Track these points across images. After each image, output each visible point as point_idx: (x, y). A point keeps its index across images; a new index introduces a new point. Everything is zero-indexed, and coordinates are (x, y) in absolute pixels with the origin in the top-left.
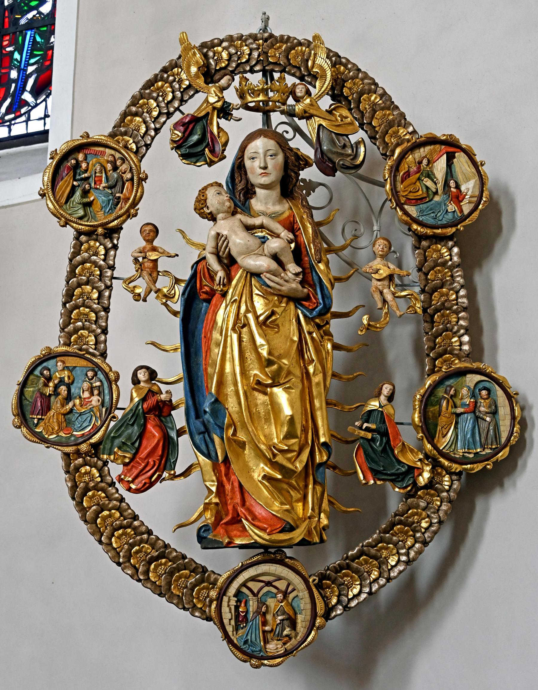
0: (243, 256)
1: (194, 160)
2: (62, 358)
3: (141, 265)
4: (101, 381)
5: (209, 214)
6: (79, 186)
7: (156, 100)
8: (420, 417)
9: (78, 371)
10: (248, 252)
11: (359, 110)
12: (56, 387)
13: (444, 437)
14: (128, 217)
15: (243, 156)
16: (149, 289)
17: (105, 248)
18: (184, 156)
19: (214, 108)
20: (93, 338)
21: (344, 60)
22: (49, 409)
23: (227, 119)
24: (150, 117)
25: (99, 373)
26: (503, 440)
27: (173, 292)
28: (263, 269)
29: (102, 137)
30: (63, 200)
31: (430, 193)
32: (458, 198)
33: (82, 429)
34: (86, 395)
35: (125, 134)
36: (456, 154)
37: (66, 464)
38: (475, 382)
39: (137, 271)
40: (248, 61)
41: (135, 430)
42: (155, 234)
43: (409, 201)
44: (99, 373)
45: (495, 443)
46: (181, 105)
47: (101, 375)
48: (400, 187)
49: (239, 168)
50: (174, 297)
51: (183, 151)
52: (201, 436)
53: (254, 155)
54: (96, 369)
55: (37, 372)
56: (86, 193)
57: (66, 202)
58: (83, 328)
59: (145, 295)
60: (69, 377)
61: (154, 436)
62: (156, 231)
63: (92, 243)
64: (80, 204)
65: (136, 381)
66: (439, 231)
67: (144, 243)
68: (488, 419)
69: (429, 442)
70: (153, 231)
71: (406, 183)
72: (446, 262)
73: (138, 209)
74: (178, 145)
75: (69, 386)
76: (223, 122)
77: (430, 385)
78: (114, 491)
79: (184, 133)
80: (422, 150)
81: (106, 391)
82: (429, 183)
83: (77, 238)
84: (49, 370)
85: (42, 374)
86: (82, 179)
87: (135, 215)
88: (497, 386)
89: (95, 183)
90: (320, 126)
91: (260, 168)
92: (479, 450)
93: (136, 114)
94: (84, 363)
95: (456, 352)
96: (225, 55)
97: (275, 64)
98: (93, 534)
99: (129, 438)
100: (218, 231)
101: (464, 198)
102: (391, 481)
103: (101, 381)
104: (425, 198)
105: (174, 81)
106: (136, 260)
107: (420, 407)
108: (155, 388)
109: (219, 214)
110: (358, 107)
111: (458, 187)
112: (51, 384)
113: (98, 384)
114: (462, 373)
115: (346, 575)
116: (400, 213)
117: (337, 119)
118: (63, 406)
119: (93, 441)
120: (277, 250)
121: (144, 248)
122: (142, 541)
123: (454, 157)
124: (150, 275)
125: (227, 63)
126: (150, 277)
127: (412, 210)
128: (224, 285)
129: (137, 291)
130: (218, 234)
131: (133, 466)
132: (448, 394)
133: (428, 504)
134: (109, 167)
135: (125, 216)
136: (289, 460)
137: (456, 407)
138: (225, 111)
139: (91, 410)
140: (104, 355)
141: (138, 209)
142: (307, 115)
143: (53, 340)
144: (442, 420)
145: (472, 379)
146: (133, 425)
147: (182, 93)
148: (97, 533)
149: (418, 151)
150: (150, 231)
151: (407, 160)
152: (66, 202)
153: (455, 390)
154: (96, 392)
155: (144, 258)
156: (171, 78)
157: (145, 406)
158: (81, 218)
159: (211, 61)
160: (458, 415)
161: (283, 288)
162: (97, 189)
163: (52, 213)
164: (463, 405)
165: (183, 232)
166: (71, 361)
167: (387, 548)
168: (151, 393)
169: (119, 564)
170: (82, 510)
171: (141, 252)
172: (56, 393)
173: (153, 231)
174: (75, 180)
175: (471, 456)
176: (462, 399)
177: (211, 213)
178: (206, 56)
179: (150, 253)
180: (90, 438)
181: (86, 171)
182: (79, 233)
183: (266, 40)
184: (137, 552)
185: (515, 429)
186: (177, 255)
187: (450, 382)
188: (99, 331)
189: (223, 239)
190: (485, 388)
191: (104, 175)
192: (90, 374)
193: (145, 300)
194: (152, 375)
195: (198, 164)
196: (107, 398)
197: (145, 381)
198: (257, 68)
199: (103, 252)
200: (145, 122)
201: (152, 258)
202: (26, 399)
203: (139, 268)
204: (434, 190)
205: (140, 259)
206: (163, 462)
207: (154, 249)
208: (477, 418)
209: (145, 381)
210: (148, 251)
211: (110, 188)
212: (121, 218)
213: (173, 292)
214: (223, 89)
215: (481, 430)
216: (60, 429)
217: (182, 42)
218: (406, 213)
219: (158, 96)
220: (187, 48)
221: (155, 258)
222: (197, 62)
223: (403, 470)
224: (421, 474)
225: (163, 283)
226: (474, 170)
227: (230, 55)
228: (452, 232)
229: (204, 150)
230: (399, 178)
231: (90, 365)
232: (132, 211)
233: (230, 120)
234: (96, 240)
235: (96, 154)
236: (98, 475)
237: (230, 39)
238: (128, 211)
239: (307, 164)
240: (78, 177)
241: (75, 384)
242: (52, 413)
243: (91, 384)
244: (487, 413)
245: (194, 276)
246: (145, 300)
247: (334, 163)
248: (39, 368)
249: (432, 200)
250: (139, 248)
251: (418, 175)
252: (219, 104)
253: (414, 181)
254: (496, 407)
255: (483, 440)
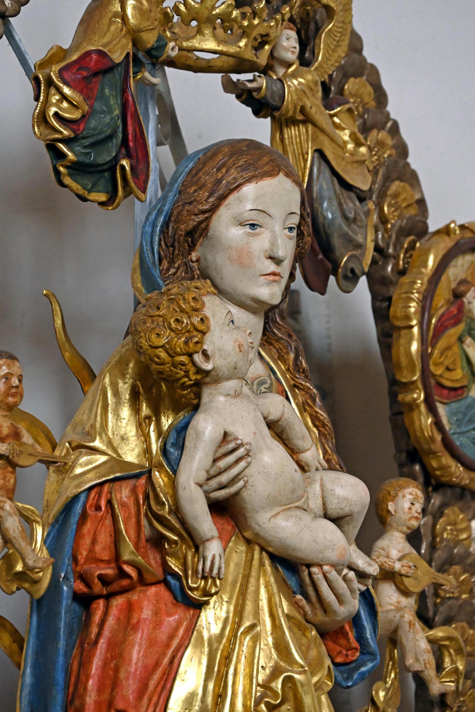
0: (278, 509)
5: (199, 371)
10: (293, 502)
15: (214, 209)
91: (271, 258)
100: (230, 429)
109: (229, 378)
189: (241, 451)
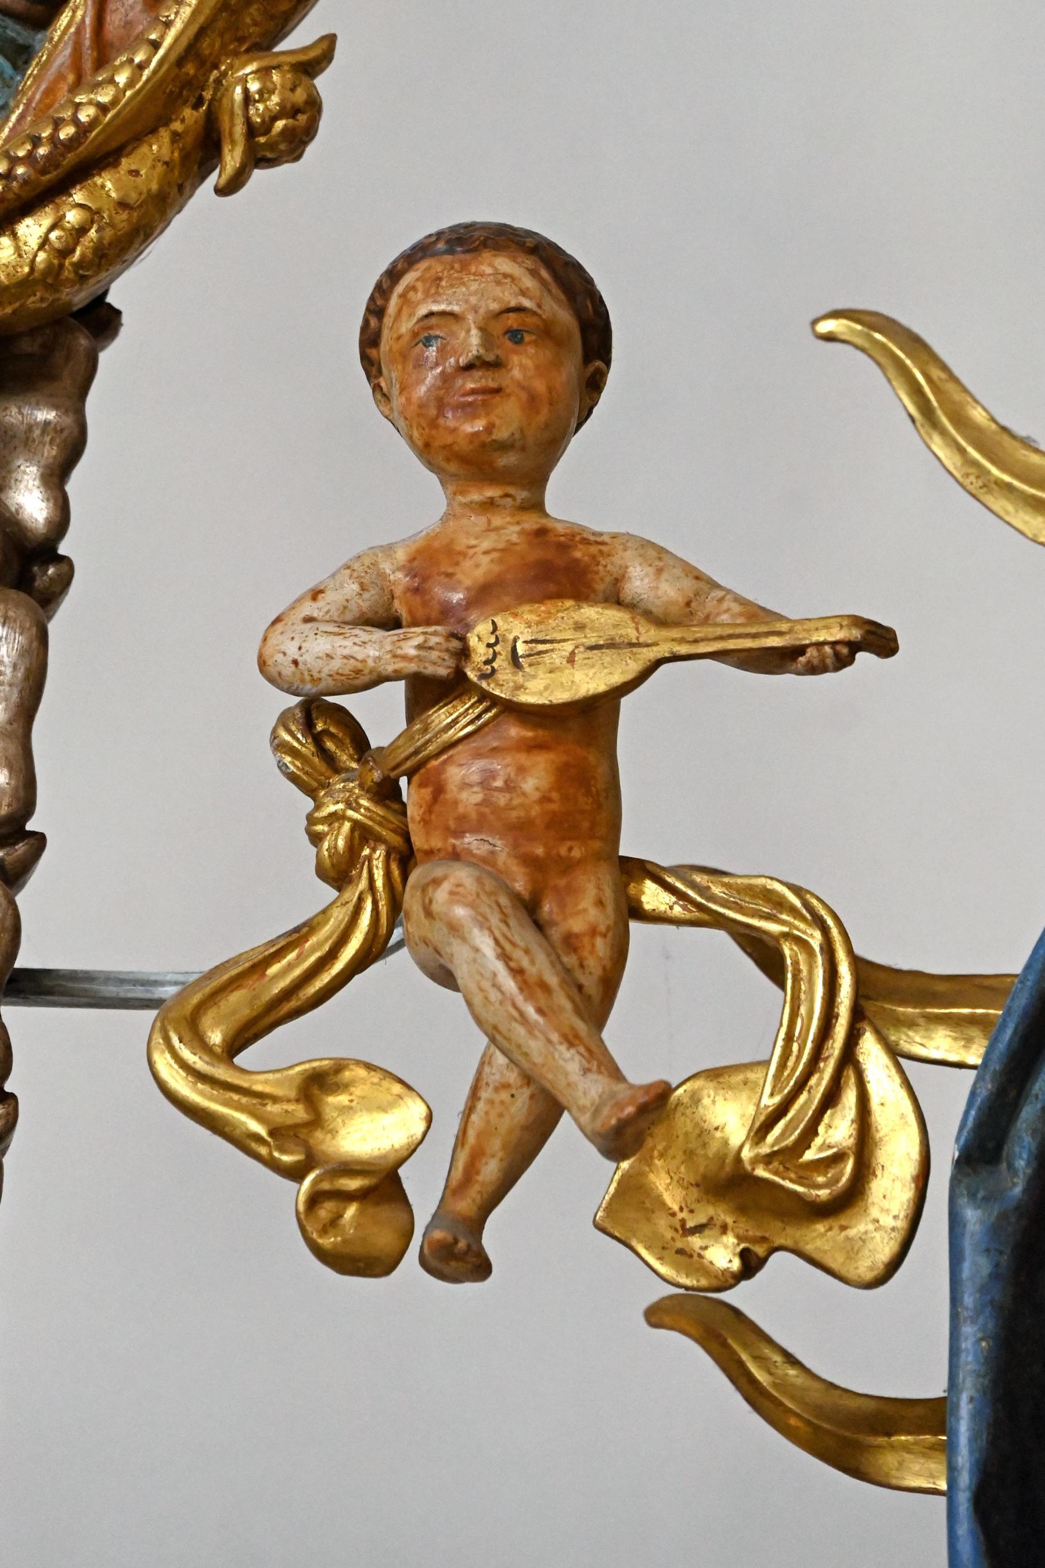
3: (387, 793)
14: (203, 152)
16: (520, 1107)
27: (839, 1130)
39: (338, 873)
42: (570, 371)
50: (851, 1197)
59: (453, 1191)
62: (577, 328)
67: (413, 502)
70: (547, 332)
73: (330, 40)
87: (287, 137)
121: (429, 561)
124: (530, 908)
126: (523, 935)
129: (365, 1133)
135: (159, 147)
141: (330, 40)
150: (511, 328)
155: (425, 693)
165: (915, 343)
171: (391, 623)
173: (547, 332)
179: (518, 628)
186: (881, 641)
193: (460, 1258)
201: (537, 690)
203: (362, 835)
205: (381, 715)
207: (565, 571)
210: (484, 595)
212: (108, 183)
213: (839, 1130)
221: (589, 680)
225: (688, 1014)
232: (247, 84)
246: (460, 1258)
250: (363, 569)
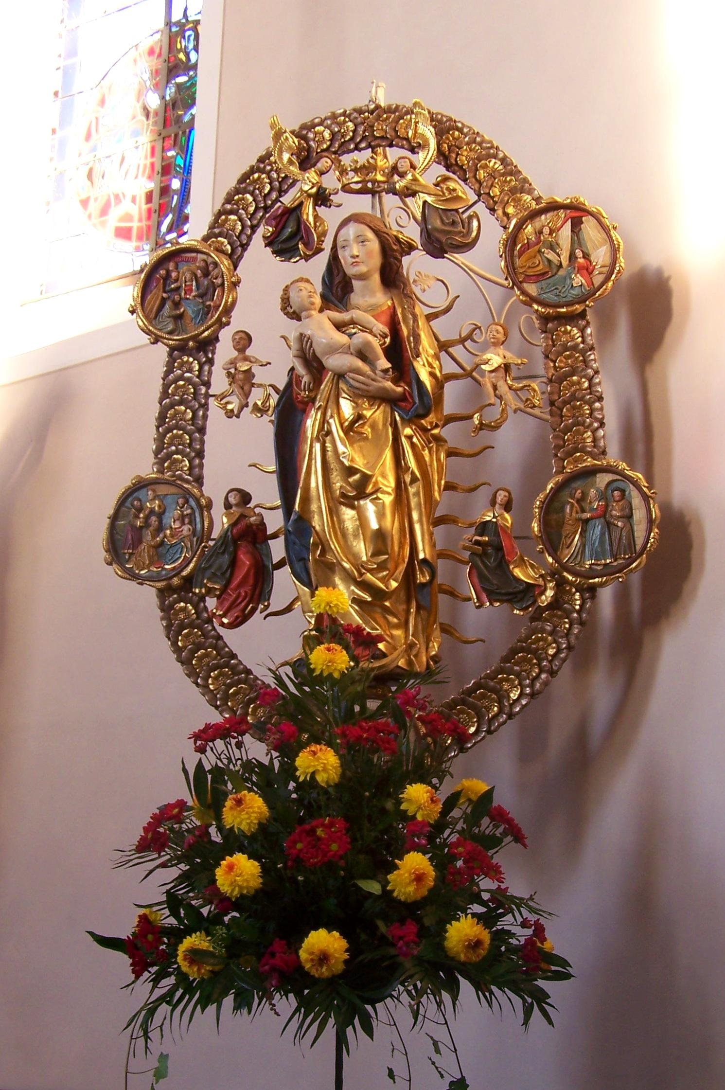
1: (288, 255)
2: (153, 487)
3: (233, 378)
4: (192, 509)
6: (169, 298)
7: (252, 194)
8: (539, 526)
9: (169, 499)
11: (476, 179)
12: (147, 518)
13: (568, 548)
17: (199, 363)
18: (277, 253)
19: (309, 196)
20: (187, 463)
21: (460, 125)
22: (140, 542)
23: (326, 206)
24: (246, 214)
25: (191, 499)
26: (638, 547)
28: (345, 368)
29: (193, 242)
30: (152, 316)
31: (553, 266)
32: (588, 270)
33: (174, 562)
34: (177, 525)
35: (220, 235)
36: (584, 219)
37: (160, 602)
38: (606, 482)
40: (352, 139)
41: (226, 559)
43: (528, 278)
44: (191, 499)
45: (628, 551)
46: (281, 196)
47: (193, 503)
48: (518, 262)
49: (334, 261)
50: (268, 410)
51: (278, 247)
52: (301, 563)
53: (345, 244)
54: (188, 496)
55: (128, 504)
56: (177, 305)
57: (155, 318)
58: (177, 452)
60: (159, 506)
61: (244, 564)
62: (249, 338)
63: (185, 359)
64: (169, 317)
65: (228, 506)
66: (564, 310)
68: (620, 524)
69: (549, 555)
71: (523, 258)
72: (577, 345)
74: (270, 242)
75: (160, 516)
76: (322, 211)
77: (552, 488)
78: (210, 628)
79: (276, 227)
80: (543, 217)
81: (198, 519)
82: (551, 256)
83: (170, 355)
84: (140, 500)
85: (133, 505)
86: (172, 290)
87: (228, 324)
88: (631, 486)
89: (185, 293)
90: (425, 202)
92: (608, 561)
93: (231, 212)
94: (173, 490)
95: (589, 449)
96: (327, 134)
97: (382, 138)
98: (189, 676)
99: (220, 567)
101: (594, 269)
102: (508, 601)
103: (192, 509)
104: (547, 272)
105: (272, 170)
106: (229, 374)
107: (540, 515)
108: (246, 512)
110: (475, 176)
111: (586, 256)
112: (142, 515)
113: (189, 511)
114: (592, 472)
115: (461, 712)
116: (518, 293)
117: (444, 193)
118: (154, 537)
119: (184, 573)
120: (360, 346)
121: (235, 358)
122: (240, 682)
123: (582, 223)
124: (242, 388)
125: (328, 143)
126: (241, 390)
127: (532, 289)
128: (310, 391)
129: (230, 407)
130: (301, 334)
131: (224, 599)
132: (573, 498)
133: (555, 627)
134: (199, 273)
136: (382, 580)
137: (583, 511)
138: (322, 198)
139: (182, 540)
140: (199, 480)
142: (410, 191)
143: (147, 469)
144: (567, 529)
145: (603, 480)
146: (223, 553)
147: (280, 183)
148: (192, 674)
149: (538, 219)
151: (526, 231)
152: (155, 318)
153: (582, 492)
154: (187, 521)
156: (268, 168)
157: (235, 531)
158: (171, 333)
159: (312, 143)
160: (586, 521)
161: (371, 388)
162: (187, 299)
163: (142, 330)
164: (592, 510)
166: (162, 490)
167: (507, 680)
168: (243, 516)
169: (217, 707)
170: (178, 650)
172: (146, 524)
174: (165, 292)
175: (599, 568)
176: (591, 503)
177: (294, 312)
178: (305, 138)
180: (182, 571)
181: (176, 281)
182: (172, 349)
183: (372, 112)
184: (236, 693)
185: (652, 534)
186: (270, 363)
187: (577, 484)
188: (193, 454)
190: (617, 489)
191: (194, 283)
192: (181, 501)
194: (245, 497)
195: (293, 260)
196: (199, 526)
197: (236, 505)
198: (363, 145)
199: (197, 367)
200: (241, 220)
202: (117, 533)
204: (556, 262)
206: (257, 592)
207: (246, 359)
208: (609, 525)
209: (236, 505)
211: (201, 296)
214: (322, 173)
215: (613, 538)
216: (152, 563)
217: (273, 126)
218: (524, 292)
219: (255, 189)
220: (278, 135)
222: (290, 147)
223: (521, 588)
224: (543, 592)
225: (257, 397)
226: (604, 235)
227: (333, 135)
228: (580, 310)
229: (298, 244)
230: (516, 252)
231: (181, 491)
233: (330, 207)
234: (189, 356)
235: (187, 261)
236: (193, 611)
237: (334, 117)
238: (219, 319)
239: (410, 248)
240: (167, 289)
241: (167, 514)
242: (144, 545)
243: (182, 512)
244: (619, 517)
245: (289, 385)
246: (238, 416)
247: (440, 242)
248: (130, 499)
249: (556, 273)
251: (537, 248)
252: (314, 190)
253: (533, 254)
254: (631, 509)
255: (615, 548)
